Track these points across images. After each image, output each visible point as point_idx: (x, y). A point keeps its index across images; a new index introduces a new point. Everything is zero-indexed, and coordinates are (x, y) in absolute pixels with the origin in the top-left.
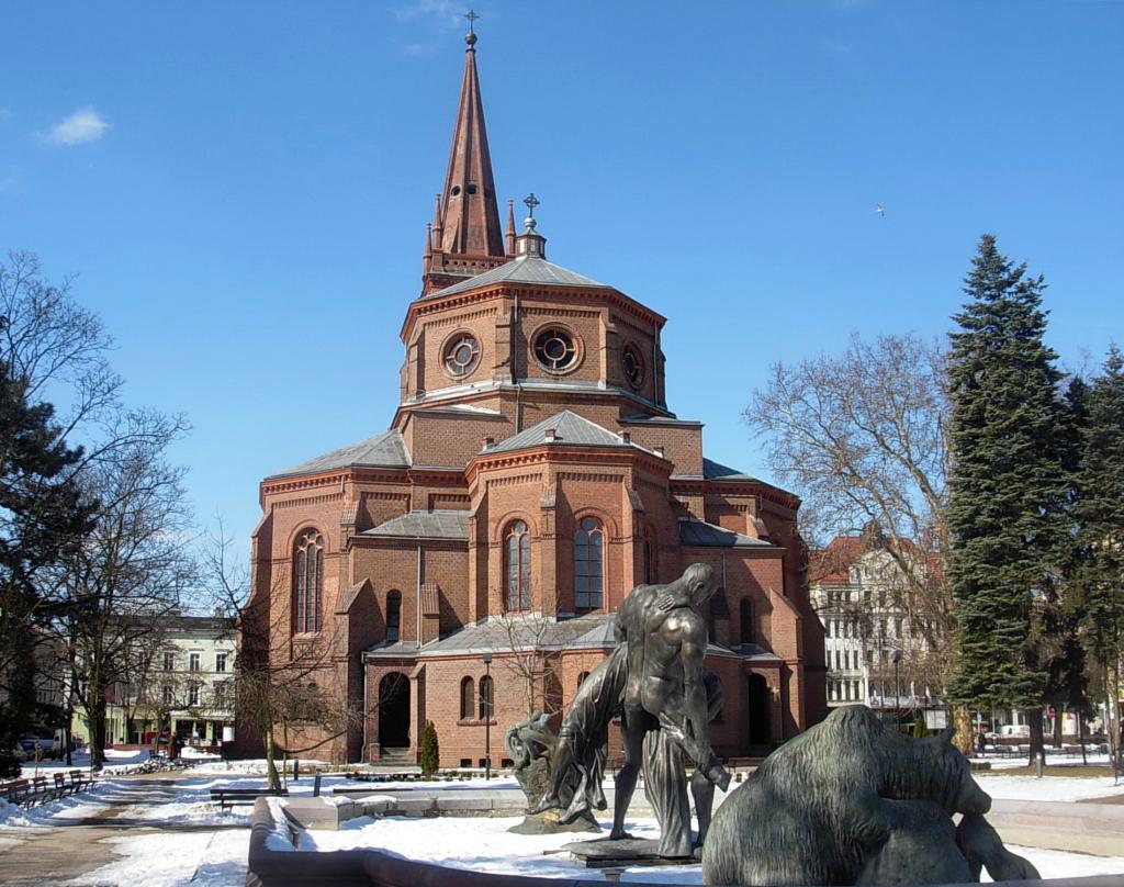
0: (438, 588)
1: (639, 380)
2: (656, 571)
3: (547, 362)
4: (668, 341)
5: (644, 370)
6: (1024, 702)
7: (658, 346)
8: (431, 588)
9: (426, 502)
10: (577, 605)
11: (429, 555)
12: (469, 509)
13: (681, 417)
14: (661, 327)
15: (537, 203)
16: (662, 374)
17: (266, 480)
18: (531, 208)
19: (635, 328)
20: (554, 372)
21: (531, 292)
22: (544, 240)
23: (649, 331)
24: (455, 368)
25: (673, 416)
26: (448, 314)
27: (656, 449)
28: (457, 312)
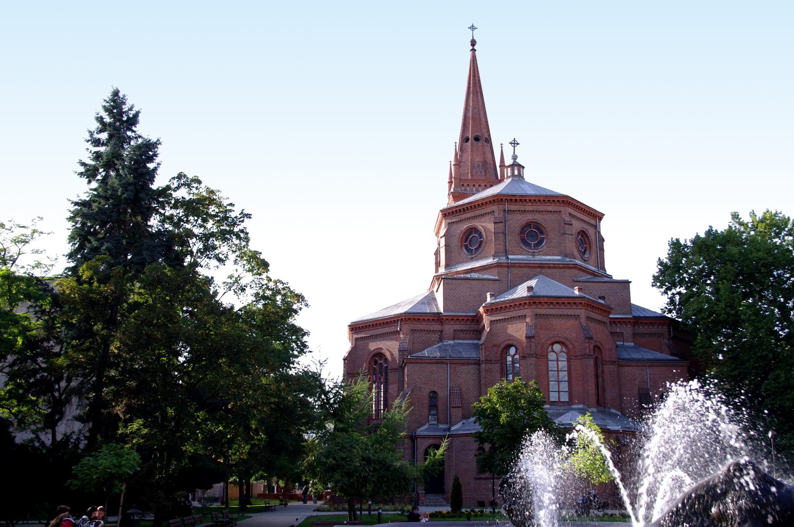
2: (603, 377)
3: (529, 245)
4: (606, 228)
5: (590, 247)
7: (599, 232)
11: (455, 369)
12: (479, 339)
13: (616, 277)
14: (600, 219)
16: (602, 250)
19: (582, 220)
22: (523, 167)
23: (593, 222)
24: (468, 250)
25: (610, 277)
26: (464, 216)
27: (600, 298)
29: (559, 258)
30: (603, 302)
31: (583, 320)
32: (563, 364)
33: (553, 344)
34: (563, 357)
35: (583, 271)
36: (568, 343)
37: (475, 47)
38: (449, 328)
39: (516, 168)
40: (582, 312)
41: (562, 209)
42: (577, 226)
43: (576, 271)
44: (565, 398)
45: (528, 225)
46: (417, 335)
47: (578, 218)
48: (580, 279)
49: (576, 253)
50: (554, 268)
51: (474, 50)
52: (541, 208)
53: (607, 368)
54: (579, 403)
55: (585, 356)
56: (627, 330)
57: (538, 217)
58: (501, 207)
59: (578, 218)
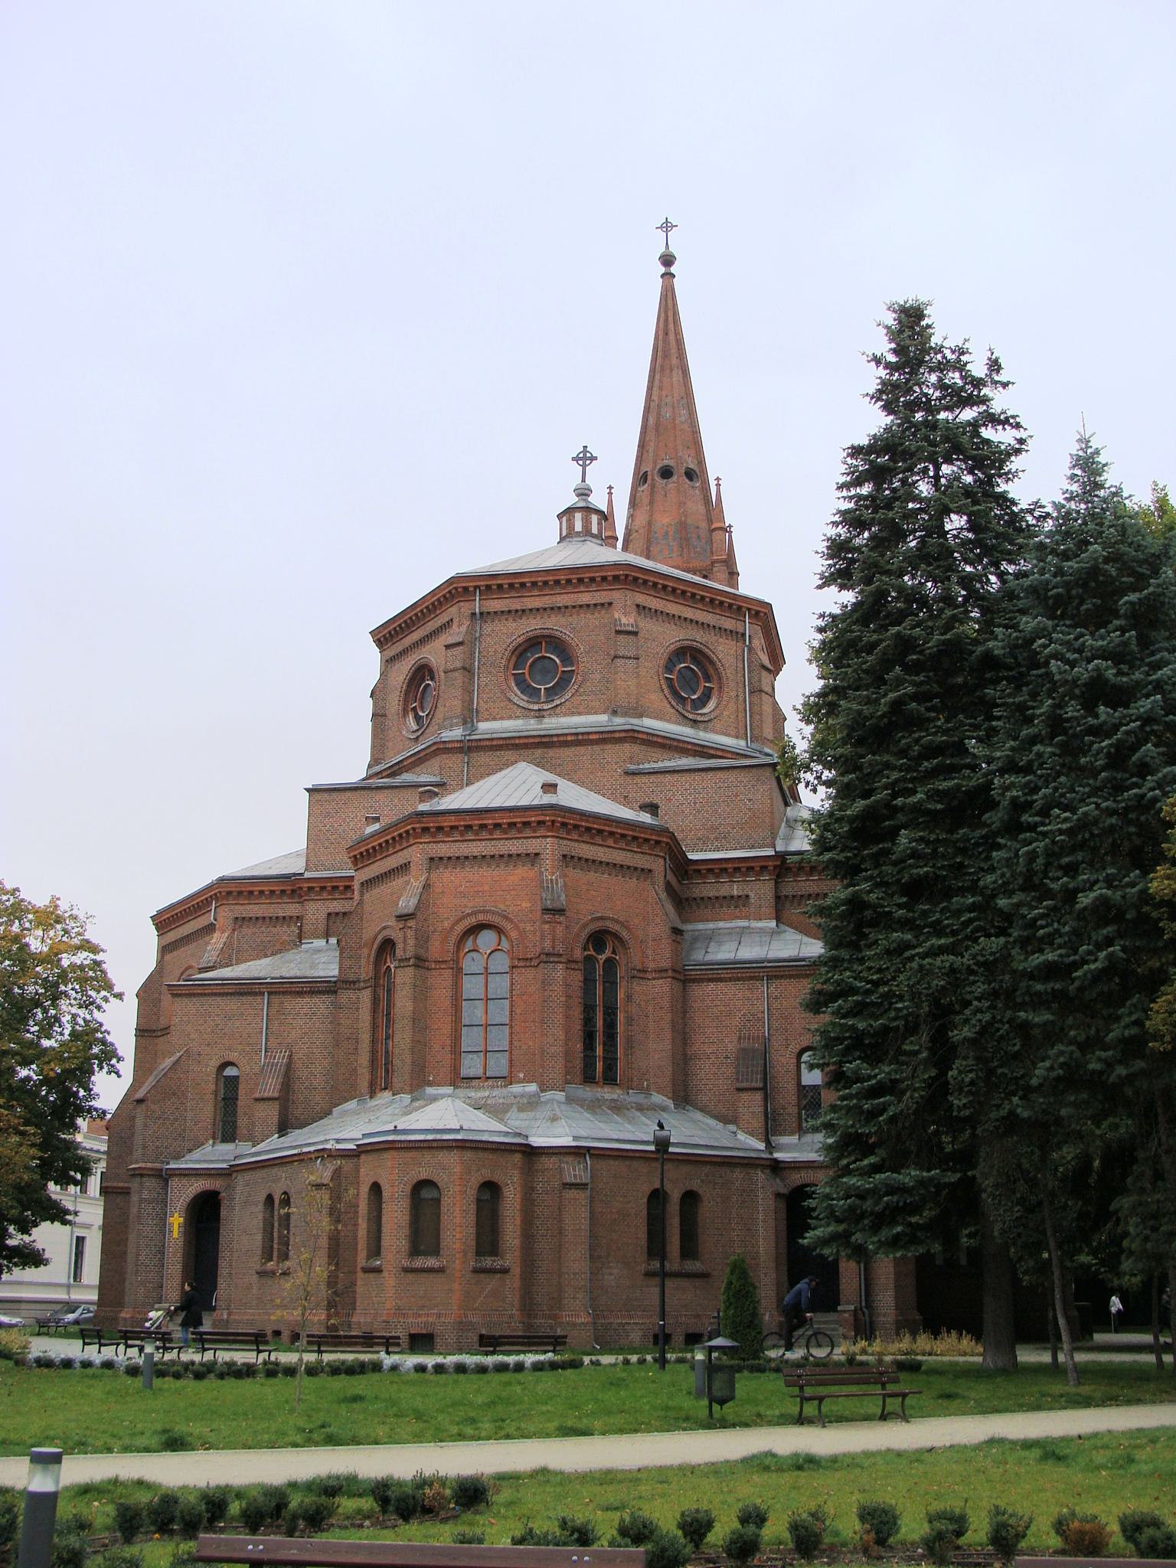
1: (712, 704)
6: (894, 1243)
8: (280, 1058)
9: (322, 927)
10: (464, 1072)
15: (593, 458)
17: (160, 913)
18: (584, 467)
20: (536, 707)
21: (500, 586)
23: (729, 624)
24: (418, 718)
28: (415, 636)
29: (601, 719)
30: (646, 818)
31: (549, 860)
32: (500, 985)
34: (501, 962)
35: (663, 746)
36: (508, 926)
37: (673, 270)
38: (316, 911)
39: (578, 516)
40: (548, 846)
41: (617, 596)
42: (666, 637)
44: (499, 1064)
45: (533, 643)
47: (671, 617)
48: (646, 766)
49: (657, 698)
50: (578, 743)
51: (668, 276)
52: (562, 600)
53: (638, 987)
54: (528, 1080)
55: (548, 957)
56: (761, 890)
57: (553, 624)
58: (465, 608)
59: (671, 617)
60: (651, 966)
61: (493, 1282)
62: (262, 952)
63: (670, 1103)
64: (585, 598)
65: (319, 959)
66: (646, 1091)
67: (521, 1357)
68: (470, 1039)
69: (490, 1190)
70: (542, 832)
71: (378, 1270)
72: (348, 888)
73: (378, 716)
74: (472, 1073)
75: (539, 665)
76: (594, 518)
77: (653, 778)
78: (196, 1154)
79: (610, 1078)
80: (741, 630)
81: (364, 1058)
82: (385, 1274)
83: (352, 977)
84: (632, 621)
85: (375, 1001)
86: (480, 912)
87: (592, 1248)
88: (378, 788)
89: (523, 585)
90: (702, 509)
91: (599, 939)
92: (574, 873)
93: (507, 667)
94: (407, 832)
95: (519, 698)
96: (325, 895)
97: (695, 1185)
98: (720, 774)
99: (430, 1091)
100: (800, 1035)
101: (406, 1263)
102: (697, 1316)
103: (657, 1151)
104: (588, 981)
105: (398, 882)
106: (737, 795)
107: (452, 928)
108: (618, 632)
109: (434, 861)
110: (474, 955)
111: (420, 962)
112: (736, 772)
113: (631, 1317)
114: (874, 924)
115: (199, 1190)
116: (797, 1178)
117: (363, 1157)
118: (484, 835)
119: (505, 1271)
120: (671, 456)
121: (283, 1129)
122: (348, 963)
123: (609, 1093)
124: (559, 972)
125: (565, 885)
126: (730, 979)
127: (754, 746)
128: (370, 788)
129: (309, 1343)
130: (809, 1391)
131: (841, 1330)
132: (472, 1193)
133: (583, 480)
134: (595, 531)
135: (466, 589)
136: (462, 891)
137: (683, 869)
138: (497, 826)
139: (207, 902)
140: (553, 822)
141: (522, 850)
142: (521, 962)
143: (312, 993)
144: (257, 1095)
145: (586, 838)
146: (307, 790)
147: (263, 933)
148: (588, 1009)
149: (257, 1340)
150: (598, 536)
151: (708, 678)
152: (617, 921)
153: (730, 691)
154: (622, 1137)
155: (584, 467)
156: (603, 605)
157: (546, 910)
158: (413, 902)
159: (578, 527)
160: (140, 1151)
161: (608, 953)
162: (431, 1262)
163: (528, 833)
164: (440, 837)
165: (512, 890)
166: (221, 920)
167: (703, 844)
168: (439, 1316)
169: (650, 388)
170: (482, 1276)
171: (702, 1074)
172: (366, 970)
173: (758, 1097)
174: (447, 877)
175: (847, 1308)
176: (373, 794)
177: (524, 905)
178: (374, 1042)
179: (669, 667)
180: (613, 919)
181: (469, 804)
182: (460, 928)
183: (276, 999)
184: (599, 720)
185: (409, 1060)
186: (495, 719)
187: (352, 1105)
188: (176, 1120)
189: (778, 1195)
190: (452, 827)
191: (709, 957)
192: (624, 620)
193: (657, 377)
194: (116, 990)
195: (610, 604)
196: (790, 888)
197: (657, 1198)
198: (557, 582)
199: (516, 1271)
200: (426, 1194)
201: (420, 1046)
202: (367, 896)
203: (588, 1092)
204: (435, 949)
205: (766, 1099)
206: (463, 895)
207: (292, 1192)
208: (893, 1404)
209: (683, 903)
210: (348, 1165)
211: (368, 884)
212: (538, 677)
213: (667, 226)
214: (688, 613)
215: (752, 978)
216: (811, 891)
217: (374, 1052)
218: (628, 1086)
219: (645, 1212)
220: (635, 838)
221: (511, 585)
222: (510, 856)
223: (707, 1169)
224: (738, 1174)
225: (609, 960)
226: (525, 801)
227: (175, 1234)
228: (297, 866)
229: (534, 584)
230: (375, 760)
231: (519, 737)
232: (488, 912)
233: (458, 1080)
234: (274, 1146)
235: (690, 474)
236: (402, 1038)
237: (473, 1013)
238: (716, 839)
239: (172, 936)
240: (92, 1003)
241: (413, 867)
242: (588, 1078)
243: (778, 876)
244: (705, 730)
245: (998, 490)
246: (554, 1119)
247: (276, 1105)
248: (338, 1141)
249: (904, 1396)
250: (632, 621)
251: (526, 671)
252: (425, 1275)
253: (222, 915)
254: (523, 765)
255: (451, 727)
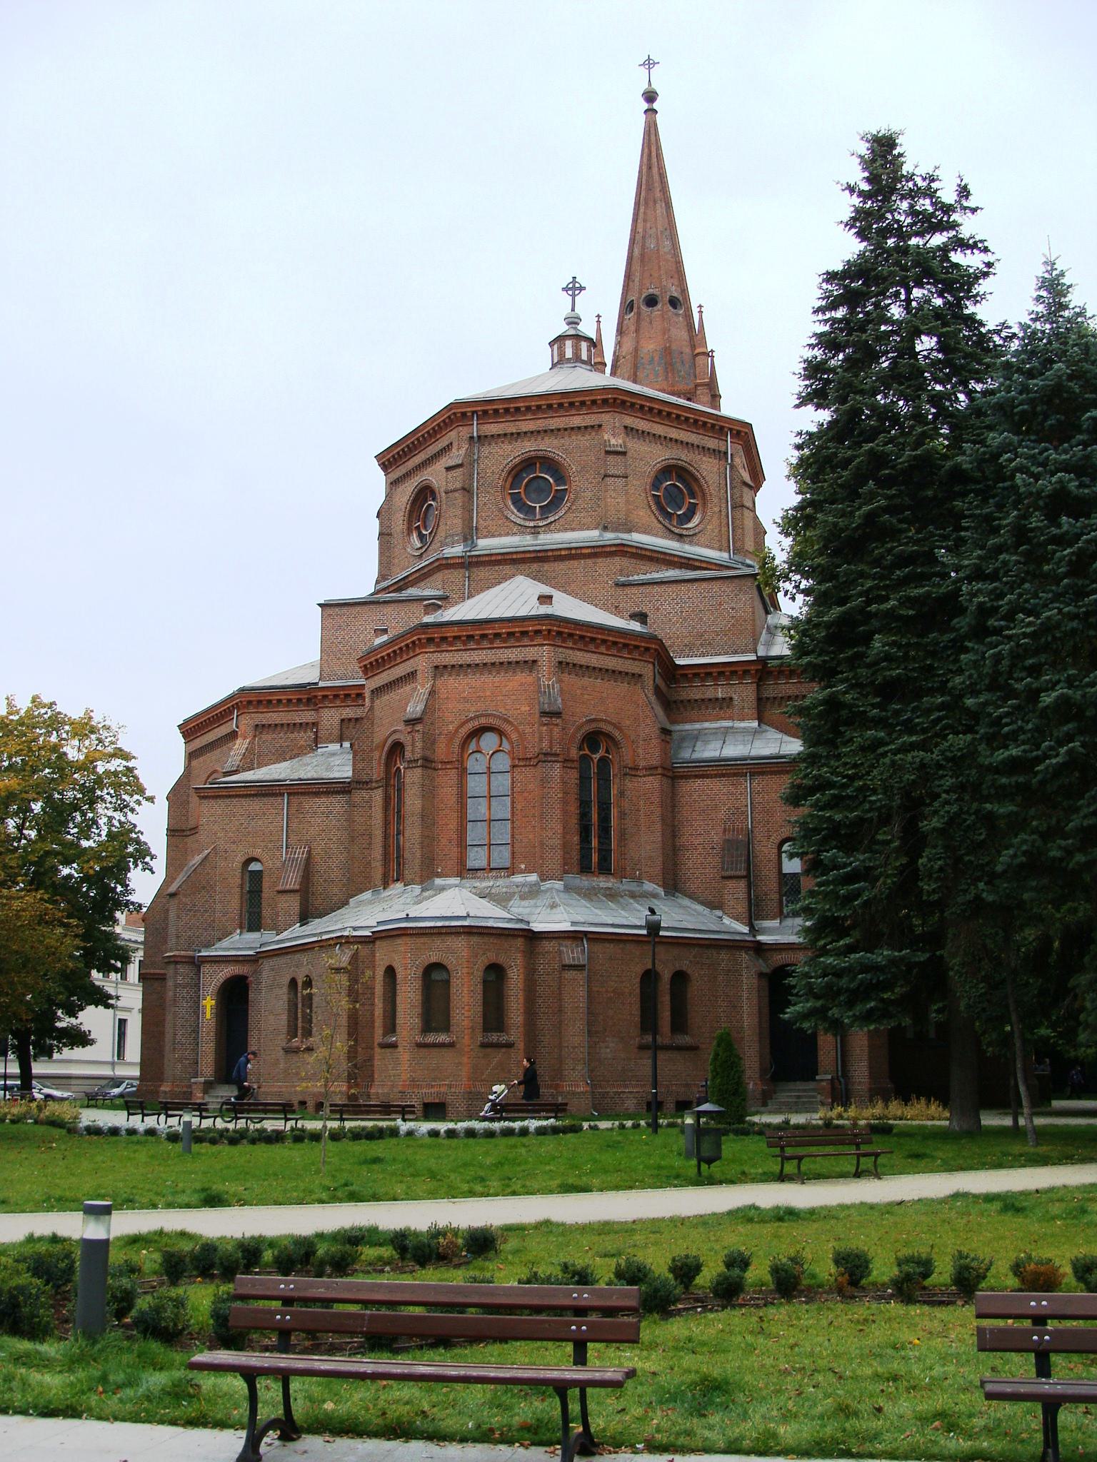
0: (309, 852)
1: (696, 520)
3: (528, 511)
5: (704, 504)
6: (868, 1017)
8: (301, 854)
9: (336, 732)
10: (470, 864)
15: (582, 289)
17: (186, 722)
18: (574, 296)
20: (532, 524)
21: (496, 411)
23: (711, 443)
24: (421, 537)
30: (635, 626)
32: (502, 783)
33: (478, 732)
34: (502, 762)
35: (651, 559)
36: (508, 728)
37: (655, 106)
38: (330, 717)
39: (569, 343)
40: (544, 654)
41: (606, 419)
42: (653, 456)
43: (625, 562)
44: (502, 857)
45: (529, 463)
46: (267, 737)
48: (636, 577)
49: (644, 514)
51: (651, 112)
53: (629, 784)
55: (545, 757)
56: (744, 693)
58: (464, 432)
60: (642, 764)
61: (497, 1056)
62: (281, 756)
63: (661, 891)
64: (577, 421)
65: (334, 762)
66: (639, 880)
67: (526, 1123)
68: (475, 834)
69: (495, 973)
70: (538, 640)
71: (394, 1046)
72: (360, 696)
73: (384, 535)
74: (477, 864)
75: (535, 484)
76: (584, 345)
77: (641, 589)
78: (225, 943)
79: (604, 868)
80: (723, 449)
81: (377, 852)
82: (400, 1049)
83: (365, 778)
84: (620, 441)
85: (387, 800)
86: (482, 715)
87: (590, 1024)
88: (385, 602)
89: (517, 409)
90: (684, 335)
91: (593, 739)
92: (569, 679)
93: (503, 487)
94: (413, 642)
95: (516, 516)
96: (338, 703)
97: (684, 965)
98: (704, 585)
99: (438, 881)
100: (781, 826)
101: (419, 1039)
102: (687, 1085)
103: (649, 935)
104: (584, 780)
105: (407, 688)
106: (720, 604)
107: (457, 731)
108: (608, 453)
109: (439, 670)
110: (478, 756)
111: (427, 763)
112: (719, 583)
113: (626, 1086)
114: (849, 723)
115: (228, 975)
116: (780, 959)
117: (378, 943)
118: (485, 644)
119: (509, 1045)
120: (656, 285)
121: (304, 918)
122: (360, 766)
123: (603, 882)
124: (556, 770)
125: (561, 690)
126: (716, 776)
127: (736, 557)
128: (378, 603)
129: (332, 1111)
130: (789, 1151)
131: (819, 1098)
132: (479, 974)
133: (573, 310)
134: (584, 357)
135: (464, 414)
136: (466, 696)
137: (671, 674)
138: (497, 635)
139: (229, 712)
140: (549, 631)
141: (520, 658)
142: (520, 762)
143: (328, 793)
144: (280, 888)
145: (580, 645)
146: (320, 605)
147: (281, 739)
148: (584, 804)
149: (285, 1110)
150: (588, 362)
151: (693, 496)
152: (609, 723)
153: (713, 508)
154: (617, 921)
155: (574, 296)
156: (593, 427)
157: (544, 713)
158: (420, 708)
159: (569, 354)
160: (174, 941)
161: (601, 753)
162: (442, 1038)
163: (526, 641)
164: (444, 647)
165: (511, 695)
166: (242, 727)
167: (689, 650)
168: (450, 1086)
169: (635, 221)
170: (489, 1050)
171: (690, 864)
172: (377, 772)
173: (742, 884)
174: (451, 684)
175: (825, 1077)
176: (381, 607)
177: (523, 709)
178: (386, 836)
179: (656, 485)
180: (605, 721)
181: (470, 616)
182: (464, 731)
183: (295, 800)
184: (591, 536)
185: (418, 855)
186: (493, 536)
187: (367, 895)
188: (206, 911)
189: (761, 975)
190: (455, 637)
191: (696, 756)
192: (613, 442)
193: (642, 210)
194: (148, 794)
195: (600, 426)
196: (771, 690)
197: (649, 978)
198: (550, 406)
199: (521, 1045)
200: (436, 976)
201: (429, 841)
202: (377, 702)
203: (585, 882)
204: (441, 751)
205: (749, 887)
206: (466, 700)
207: (314, 976)
208: (867, 1163)
209: (672, 706)
210: (364, 951)
211: (377, 692)
212: (533, 496)
213: (649, 64)
214: (674, 434)
215: (735, 775)
216: (790, 693)
217: (386, 847)
218: (622, 875)
219: (638, 991)
220: (626, 645)
221: (507, 410)
222: (509, 663)
223: (695, 951)
224: (724, 955)
225: (602, 759)
226: (522, 613)
227: (208, 1016)
228: (311, 676)
229: (528, 408)
230: (382, 577)
231: (516, 553)
232: (490, 715)
233: (464, 871)
234: (296, 934)
235: (674, 302)
236: (412, 833)
237: (477, 809)
238: (702, 645)
239: (198, 743)
240: (126, 807)
241: (419, 675)
242: (585, 868)
243: (760, 679)
244: (691, 543)
245: (966, 312)
246: (553, 906)
247: (297, 897)
248: (355, 929)
249: (877, 1155)
250: (620, 441)
251: (521, 491)
252: (436, 1050)
253: (243, 723)
254: (520, 579)
255: (452, 545)
